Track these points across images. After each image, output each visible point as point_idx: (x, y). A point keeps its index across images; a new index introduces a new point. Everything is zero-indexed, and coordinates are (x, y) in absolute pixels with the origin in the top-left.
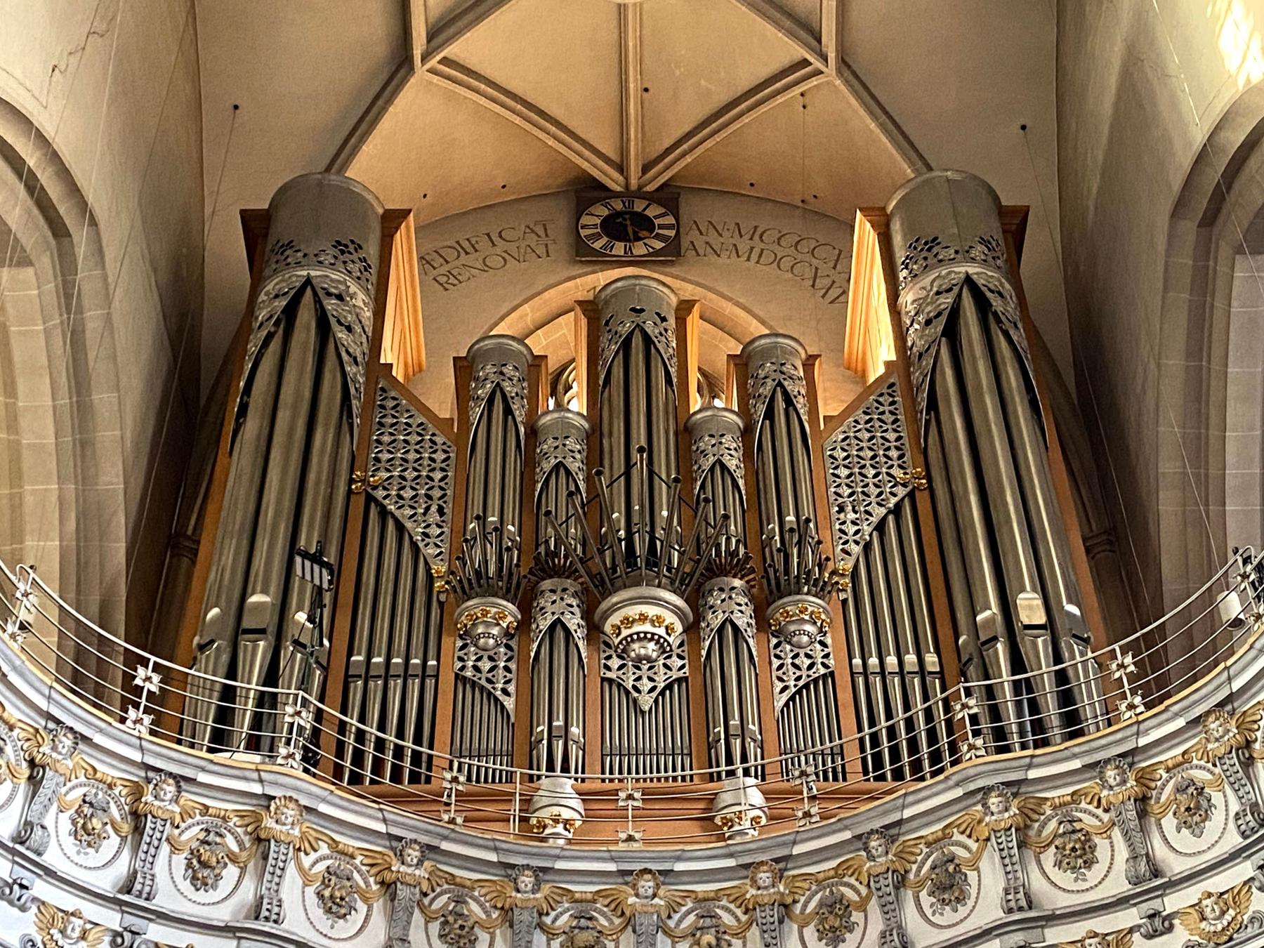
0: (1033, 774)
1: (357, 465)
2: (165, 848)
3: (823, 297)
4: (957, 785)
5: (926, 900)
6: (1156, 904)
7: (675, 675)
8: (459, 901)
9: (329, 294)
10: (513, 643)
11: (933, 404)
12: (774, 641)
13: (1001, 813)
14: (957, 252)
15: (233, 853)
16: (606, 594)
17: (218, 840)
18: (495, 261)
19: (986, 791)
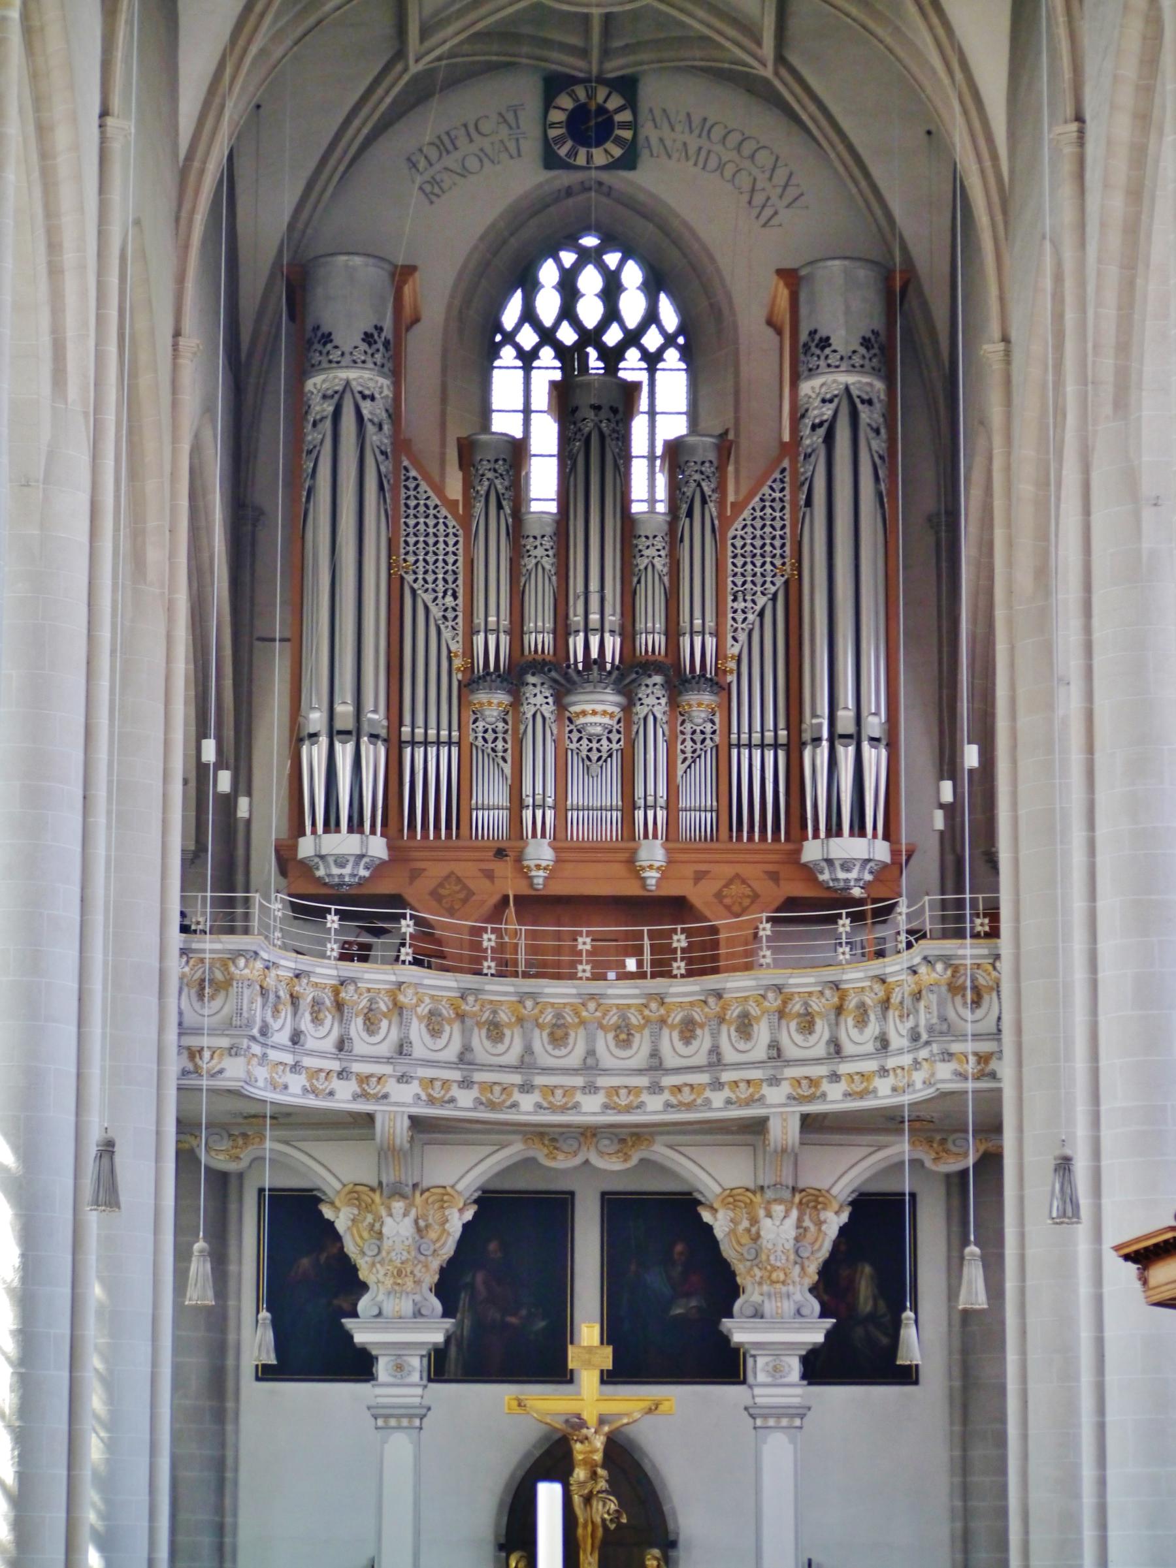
0: (792, 981)
1: (392, 552)
3: (758, 217)
4: (755, 979)
5: (733, 1034)
6: (834, 1067)
7: (615, 746)
8: (495, 1012)
9: (364, 397)
10: (509, 718)
11: (809, 503)
12: (680, 719)
13: (772, 1000)
14: (842, 358)
16: (568, 692)
17: (376, 1006)
18: (473, 163)
19: (768, 988)
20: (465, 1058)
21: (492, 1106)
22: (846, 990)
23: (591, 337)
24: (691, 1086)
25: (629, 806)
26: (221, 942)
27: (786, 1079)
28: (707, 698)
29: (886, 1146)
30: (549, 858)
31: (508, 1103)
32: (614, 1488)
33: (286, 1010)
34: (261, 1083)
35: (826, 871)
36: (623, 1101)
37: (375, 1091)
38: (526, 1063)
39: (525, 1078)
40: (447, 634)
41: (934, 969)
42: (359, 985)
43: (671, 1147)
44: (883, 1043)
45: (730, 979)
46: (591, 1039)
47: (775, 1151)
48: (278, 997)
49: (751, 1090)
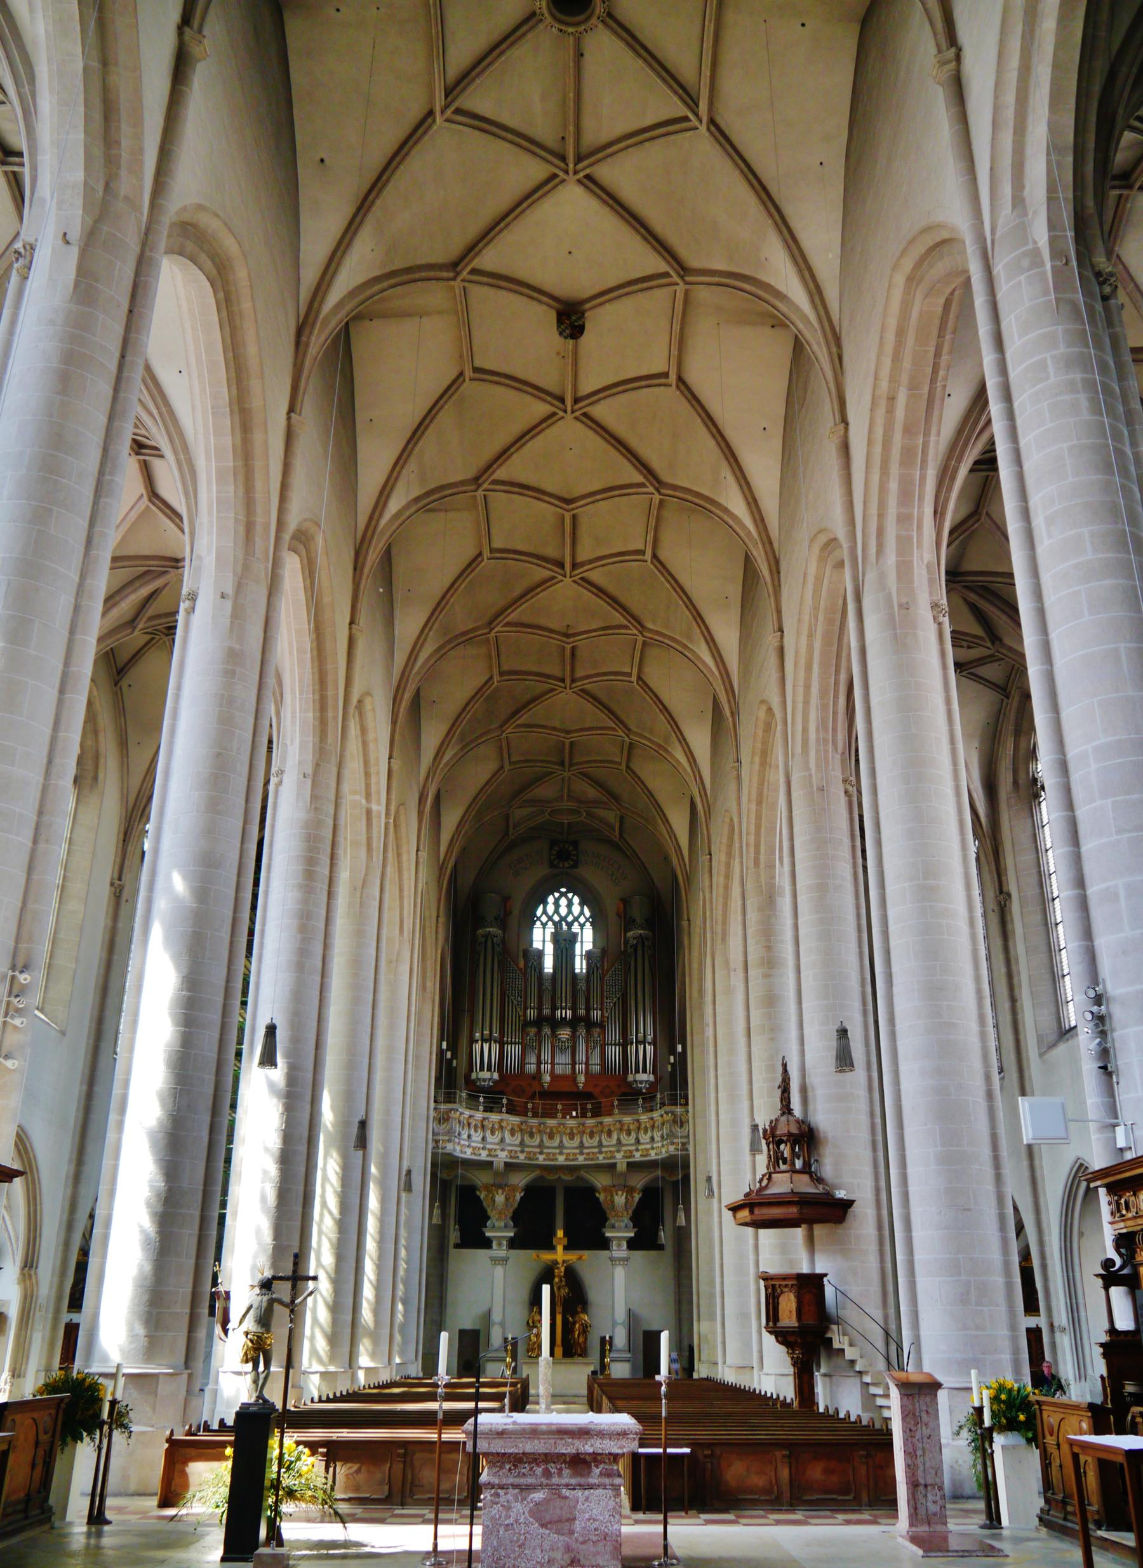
20: (522, 1143)
21: (530, 1159)
23: (563, 919)
25: (574, 1064)
28: (598, 1030)
32: (567, 1284)
33: (466, 1128)
36: (571, 1157)
38: (541, 1145)
40: (518, 1009)
44: (652, 1139)
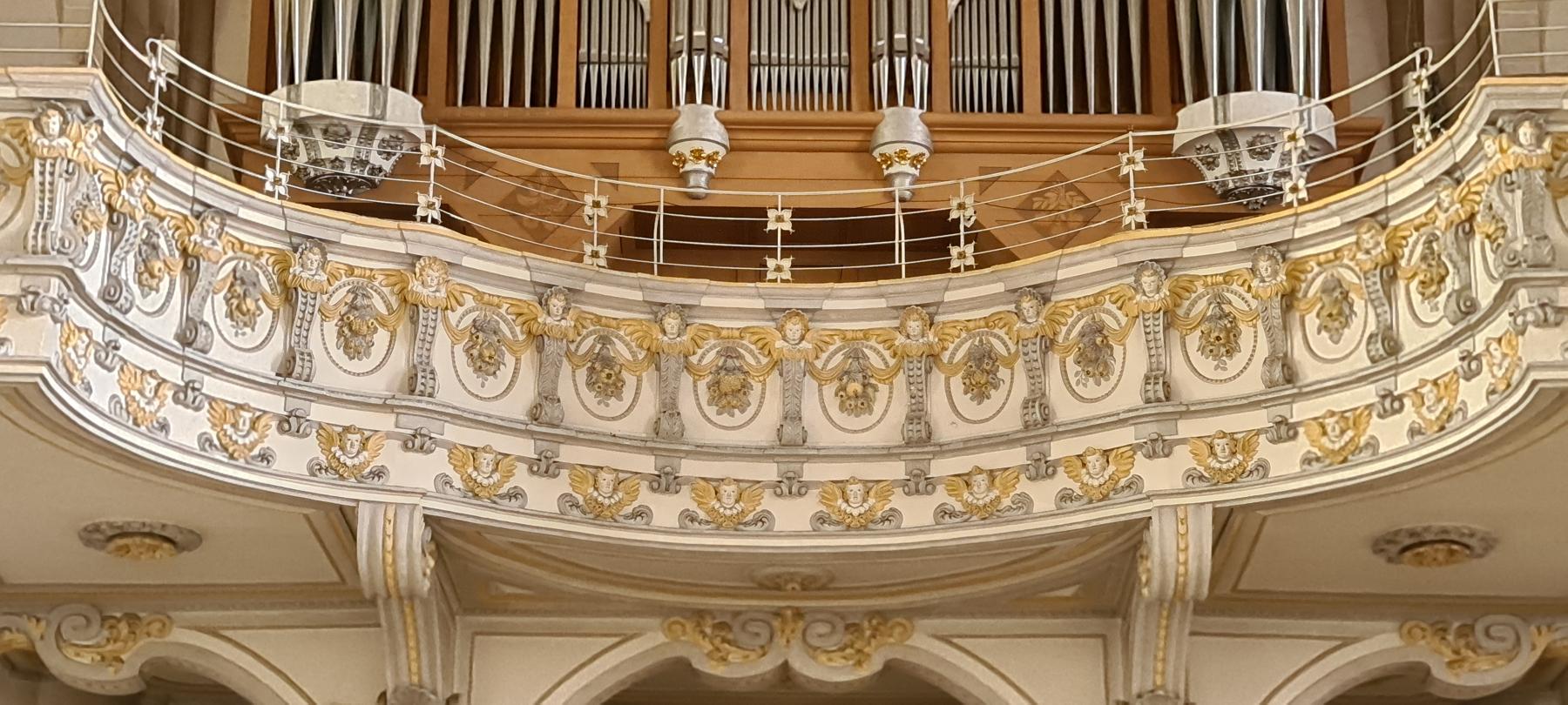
2: (318, 317)
4: (1114, 254)
5: (1072, 368)
6: (1283, 410)
8: (604, 340)
13: (1153, 292)
15: (382, 317)
17: (366, 302)
19: (1141, 266)
21: (597, 513)
22: (1305, 259)
24: (992, 474)
26: (13, 83)
27: (1183, 441)
29: (1356, 640)
30: (719, 139)
31: (628, 510)
33: (170, 280)
34: (100, 399)
35: (1222, 161)
37: (356, 461)
39: (662, 462)
41: (1514, 139)
42: (330, 256)
43: (946, 639)
45: (1065, 260)
46: (792, 393)
47: (1161, 600)
48: (155, 247)
49: (1111, 468)
